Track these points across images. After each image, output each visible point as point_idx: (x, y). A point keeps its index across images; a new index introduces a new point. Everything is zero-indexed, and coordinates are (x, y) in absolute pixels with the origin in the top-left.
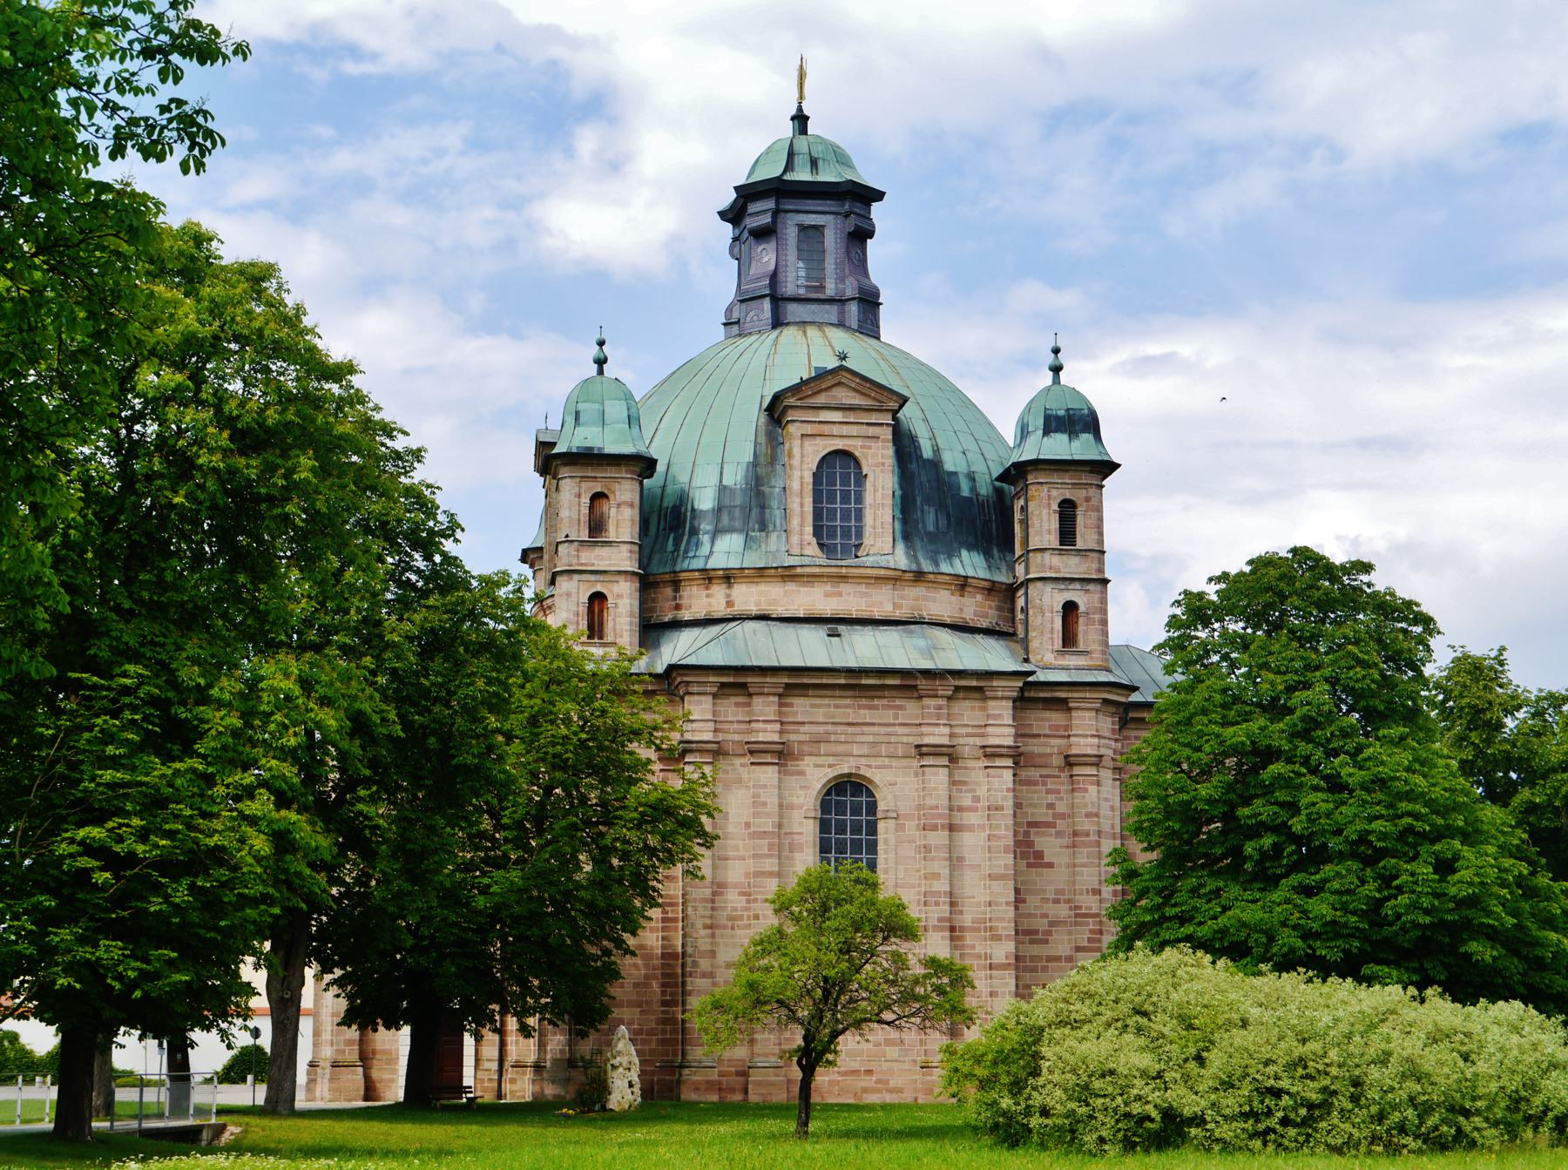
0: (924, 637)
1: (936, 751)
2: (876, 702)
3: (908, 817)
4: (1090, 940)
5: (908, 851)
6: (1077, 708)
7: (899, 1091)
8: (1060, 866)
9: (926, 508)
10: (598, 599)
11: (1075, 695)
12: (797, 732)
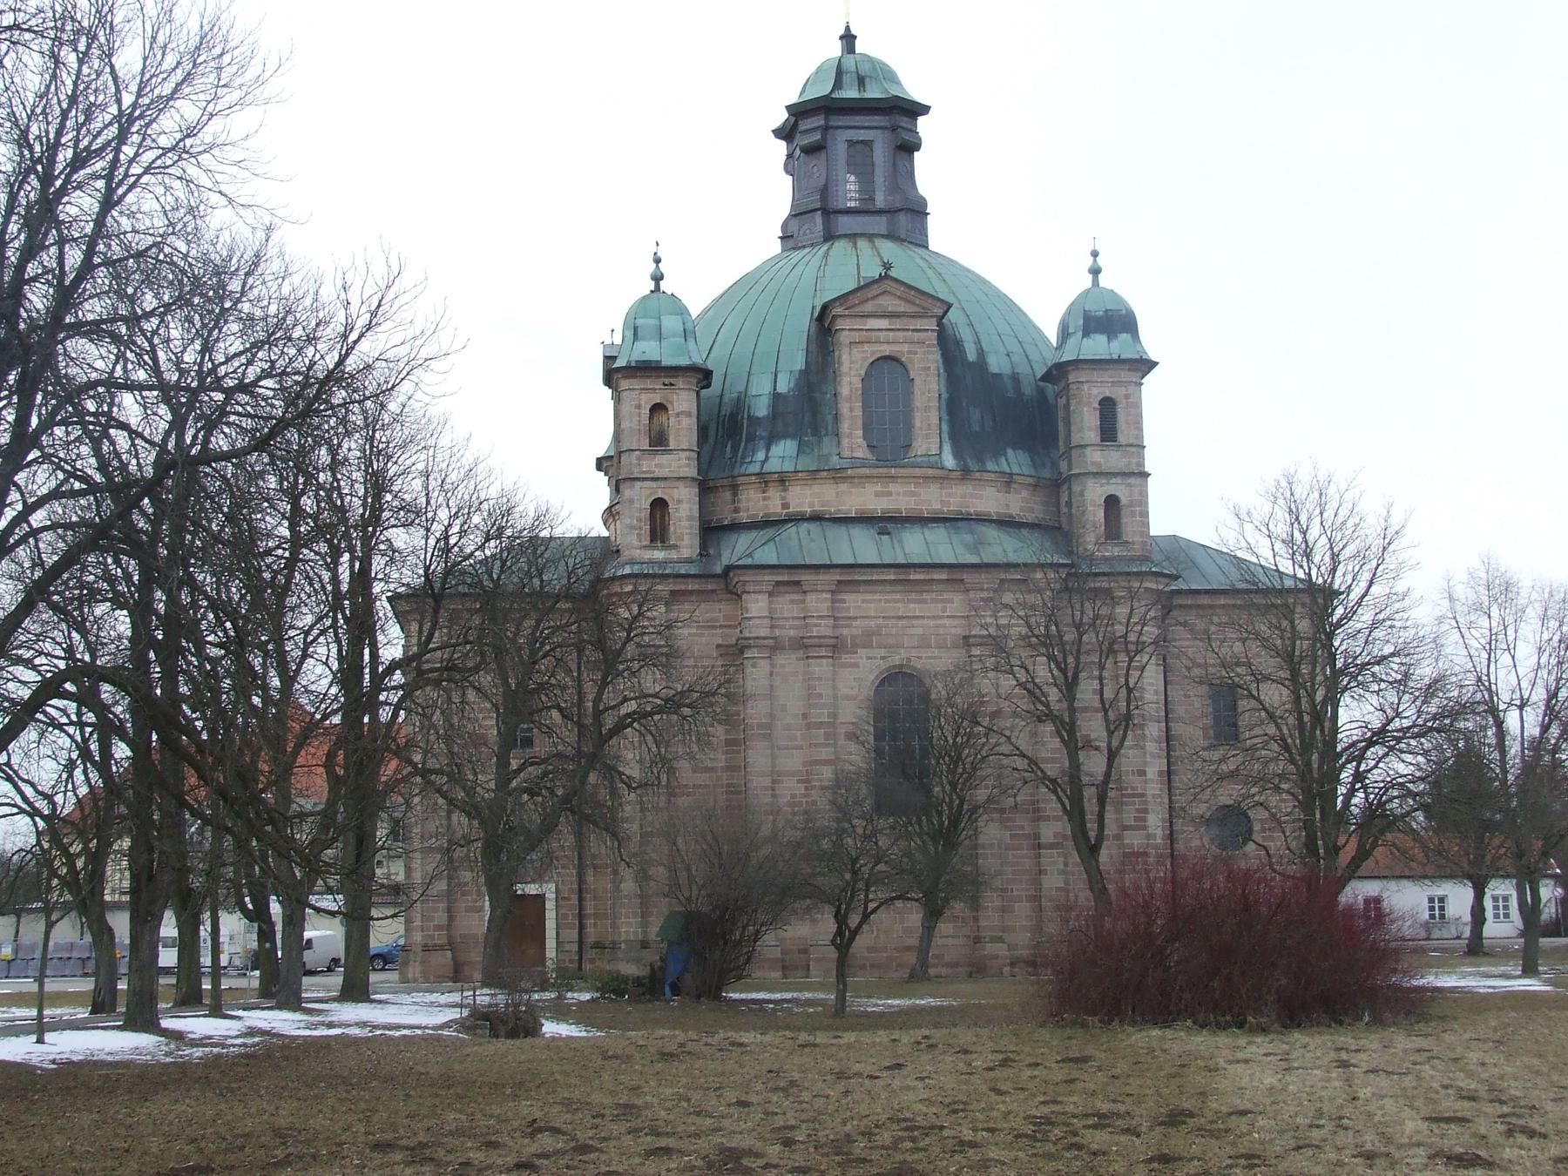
0: (972, 533)
2: (925, 596)
10: (659, 505)
12: (847, 626)
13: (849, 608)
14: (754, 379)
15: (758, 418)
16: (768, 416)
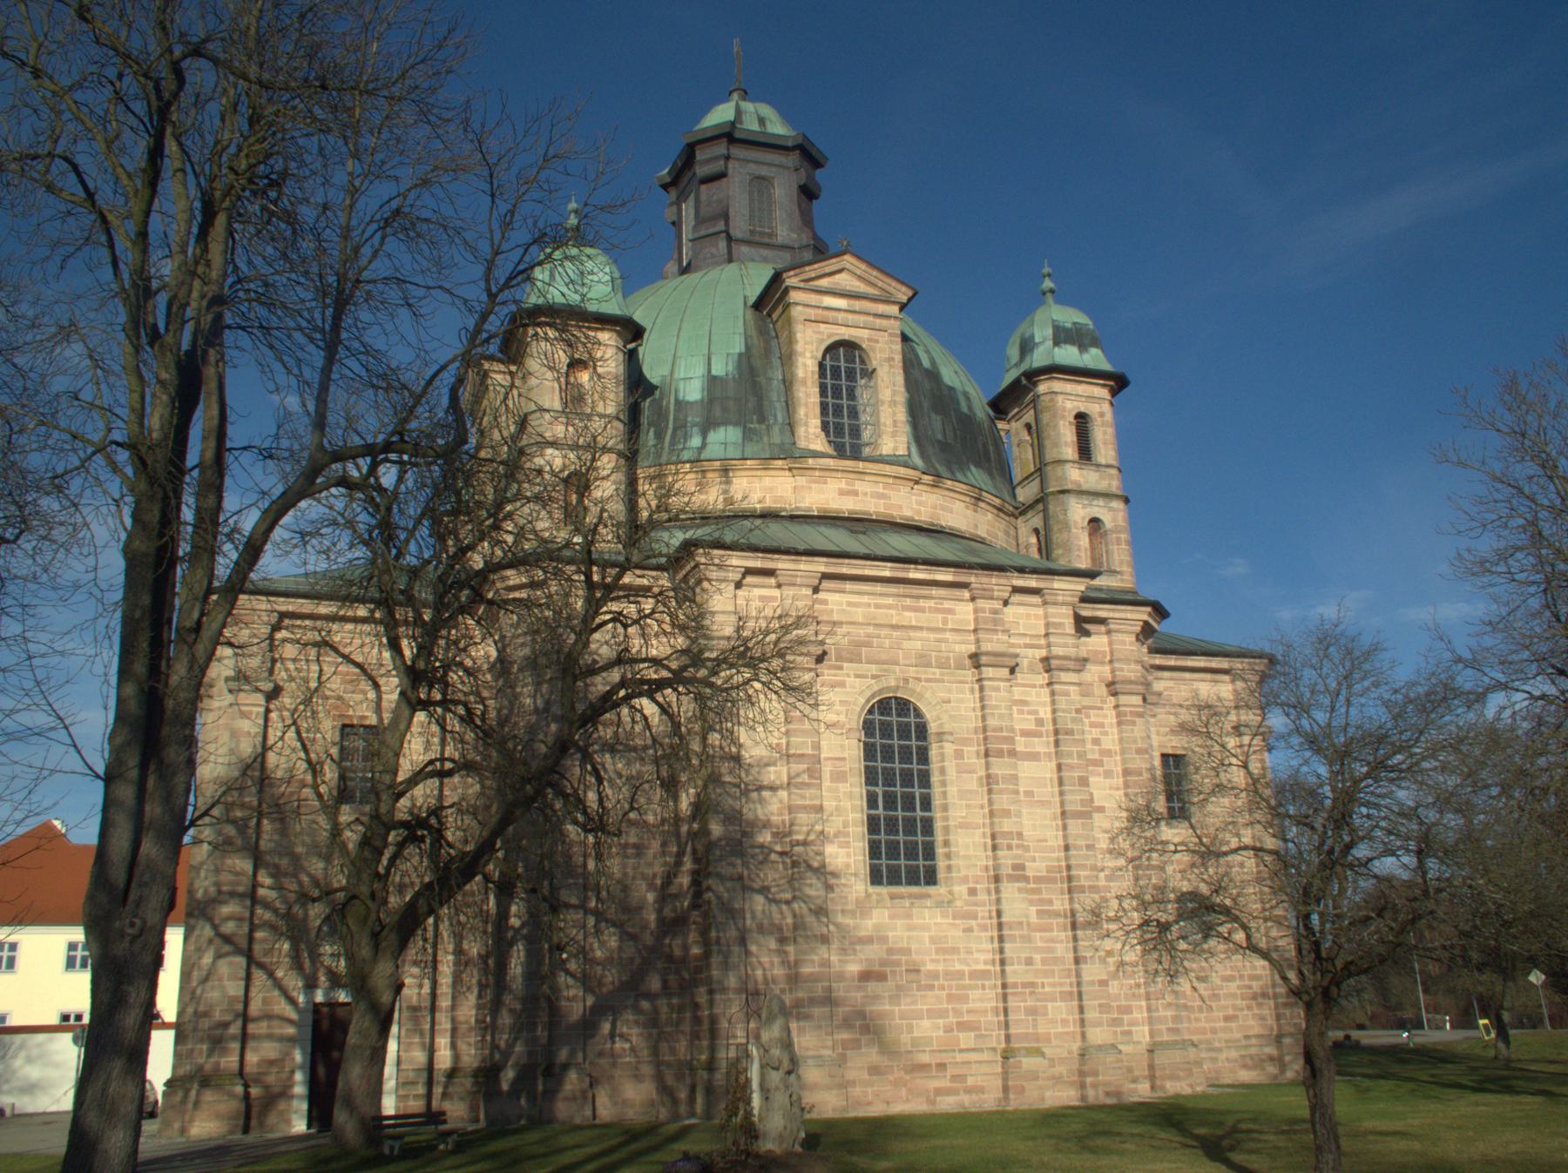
2: (922, 603)
6: (1117, 631)
7: (979, 1090)
9: (933, 416)
11: (1117, 615)
14: (682, 363)
15: (688, 403)
16: (702, 401)
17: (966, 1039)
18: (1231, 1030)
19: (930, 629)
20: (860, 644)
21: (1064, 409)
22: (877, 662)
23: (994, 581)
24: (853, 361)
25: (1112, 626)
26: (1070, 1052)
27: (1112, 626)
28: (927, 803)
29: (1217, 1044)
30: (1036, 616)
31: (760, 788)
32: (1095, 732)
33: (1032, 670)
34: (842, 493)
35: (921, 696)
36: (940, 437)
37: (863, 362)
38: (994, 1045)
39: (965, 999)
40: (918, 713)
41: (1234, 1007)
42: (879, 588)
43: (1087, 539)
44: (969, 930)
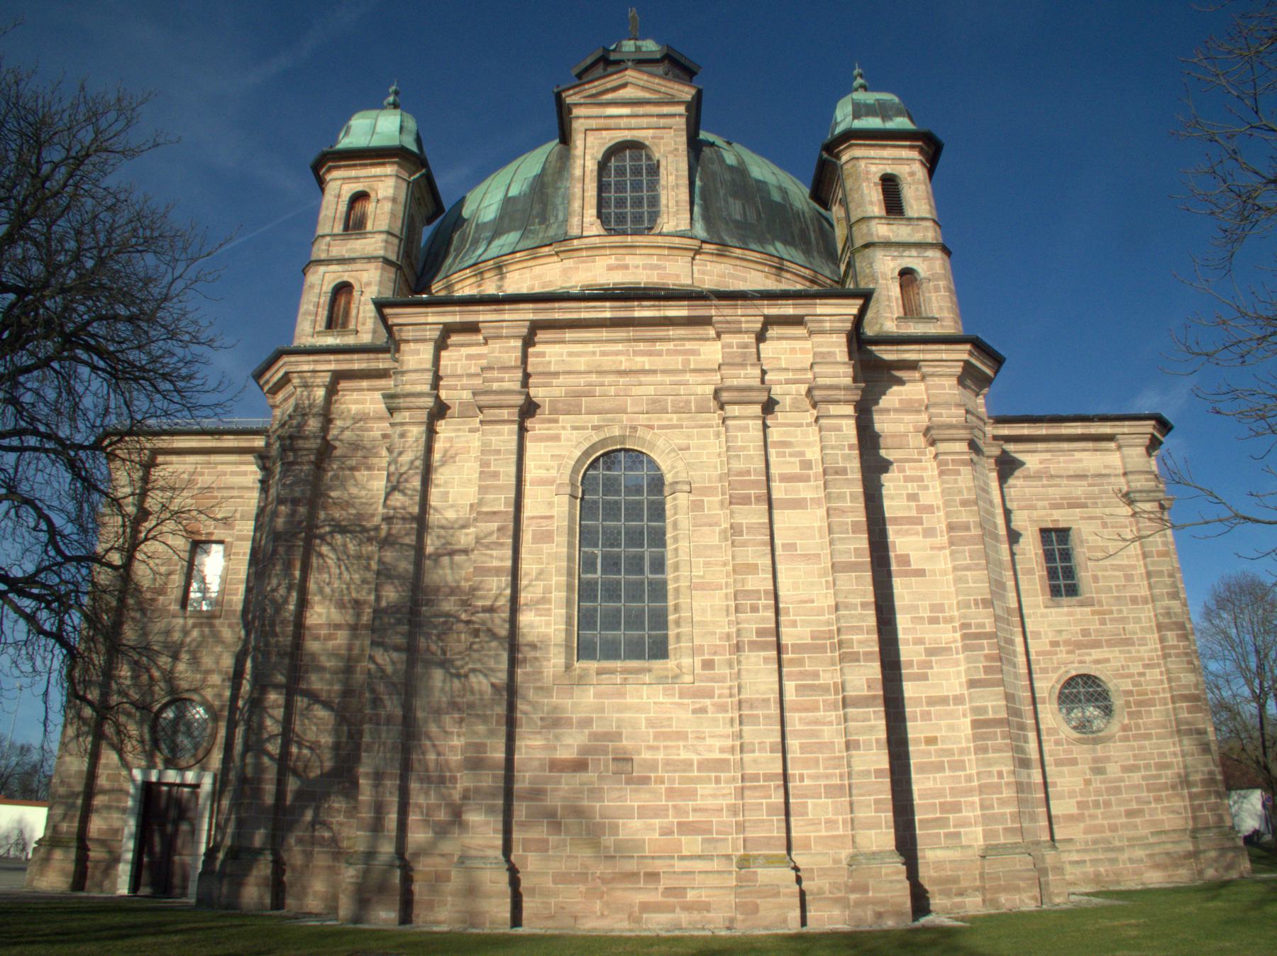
1: (742, 395)
2: (658, 346)
3: (706, 491)
4: (987, 670)
5: (712, 537)
6: (932, 375)
7: (706, 907)
8: (933, 572)
9: (731, 200)
10: (343, 289)
13: (549, 363)
17: (691, 844)
18: (1135, 827)
19: (665, 372)
20: (579, 395)
21: (868, 173)
22: (599, 413)
23: (739, 312)
24: (640, 159)
25: (924, 370)
26: (836, 861)
27: (924, 370)
28: (659, 565)
29: (1117, 843)
30: (803, 350)
31: (451, 553)
32: (912, 487)
33: (796, 408)
34: (610, 268)
35: (653, 446)
36: (738, 217)
37: (649, 158)
38: (730, 852)
39: (692, 794)
40: (653, 464)
41: (1138, 800)
42: (604, 334)
43: (898, 290)
44: (703, 710)
